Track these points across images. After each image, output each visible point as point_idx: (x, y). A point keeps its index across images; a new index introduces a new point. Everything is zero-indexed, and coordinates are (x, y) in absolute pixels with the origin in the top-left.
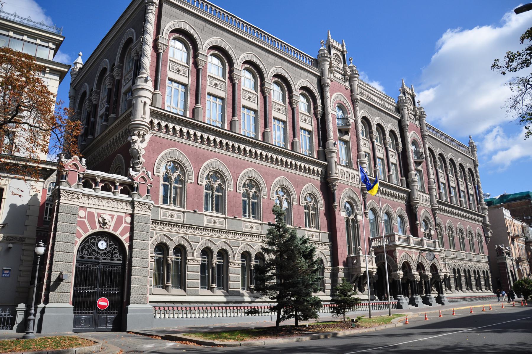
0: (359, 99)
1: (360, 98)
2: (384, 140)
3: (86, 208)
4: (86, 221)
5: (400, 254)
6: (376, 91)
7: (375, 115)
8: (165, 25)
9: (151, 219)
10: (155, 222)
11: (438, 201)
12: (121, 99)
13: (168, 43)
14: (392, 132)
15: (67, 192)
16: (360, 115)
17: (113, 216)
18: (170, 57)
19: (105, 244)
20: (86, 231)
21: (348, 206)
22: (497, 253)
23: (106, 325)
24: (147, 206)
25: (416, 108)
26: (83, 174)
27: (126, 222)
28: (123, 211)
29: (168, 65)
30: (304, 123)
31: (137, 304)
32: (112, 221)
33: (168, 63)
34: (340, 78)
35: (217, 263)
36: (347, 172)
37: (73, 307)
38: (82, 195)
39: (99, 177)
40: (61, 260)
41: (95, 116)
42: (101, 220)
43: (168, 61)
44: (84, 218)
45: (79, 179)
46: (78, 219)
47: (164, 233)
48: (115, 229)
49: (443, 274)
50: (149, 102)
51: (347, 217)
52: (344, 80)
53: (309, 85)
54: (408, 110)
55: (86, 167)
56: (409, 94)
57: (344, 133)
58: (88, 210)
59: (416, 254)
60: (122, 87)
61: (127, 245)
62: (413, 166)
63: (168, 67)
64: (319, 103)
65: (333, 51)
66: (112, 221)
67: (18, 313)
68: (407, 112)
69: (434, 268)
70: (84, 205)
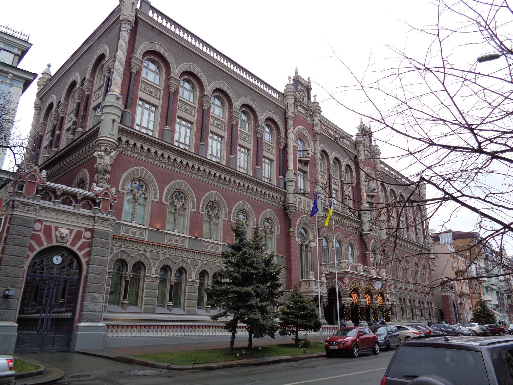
2: (340, 173)
4: (41, 234)
5: (350, 281)
7: (332, 150)
8: (140, 45)
10: (116, 238)
12: (90, 114)
13: (142, 64)
14: (348, 165)
15: (23, 204)
16: (319, 148)
17: (71, 231)
18: (142, 78)
19: (60, 259)
20: (40, 244)
21: (303, 231)
23: (53, 344)
24: (109, 222)
25: (372, 145)
26: (43, 186)
27: (85, 238)
29: (140, 85)
30: (267, 153)
32: (70, 235)
33: (140, 83)
35: (176, 281)
36: (304, 200)
37: (17, 325)
39: (60, 189)
40: (9, 275)
41: (60, 129)
43: (141, 81)
44: (40, 231)
45: (37, 190)
47: (123, 249)
48: (73, 244)
49: (390, 303)
50: (118, 120)
51: (301, 243)
53: (274, 117)
54: (364, 147)
55: (46, 180)
57: (303, 165)
58: (44, 223)
59: (365, 281)
60: (92, 102)
61: (84, 261)
63: (140, 87)
64: (283, 135)
65: (299, 87)
66: (70, 235)
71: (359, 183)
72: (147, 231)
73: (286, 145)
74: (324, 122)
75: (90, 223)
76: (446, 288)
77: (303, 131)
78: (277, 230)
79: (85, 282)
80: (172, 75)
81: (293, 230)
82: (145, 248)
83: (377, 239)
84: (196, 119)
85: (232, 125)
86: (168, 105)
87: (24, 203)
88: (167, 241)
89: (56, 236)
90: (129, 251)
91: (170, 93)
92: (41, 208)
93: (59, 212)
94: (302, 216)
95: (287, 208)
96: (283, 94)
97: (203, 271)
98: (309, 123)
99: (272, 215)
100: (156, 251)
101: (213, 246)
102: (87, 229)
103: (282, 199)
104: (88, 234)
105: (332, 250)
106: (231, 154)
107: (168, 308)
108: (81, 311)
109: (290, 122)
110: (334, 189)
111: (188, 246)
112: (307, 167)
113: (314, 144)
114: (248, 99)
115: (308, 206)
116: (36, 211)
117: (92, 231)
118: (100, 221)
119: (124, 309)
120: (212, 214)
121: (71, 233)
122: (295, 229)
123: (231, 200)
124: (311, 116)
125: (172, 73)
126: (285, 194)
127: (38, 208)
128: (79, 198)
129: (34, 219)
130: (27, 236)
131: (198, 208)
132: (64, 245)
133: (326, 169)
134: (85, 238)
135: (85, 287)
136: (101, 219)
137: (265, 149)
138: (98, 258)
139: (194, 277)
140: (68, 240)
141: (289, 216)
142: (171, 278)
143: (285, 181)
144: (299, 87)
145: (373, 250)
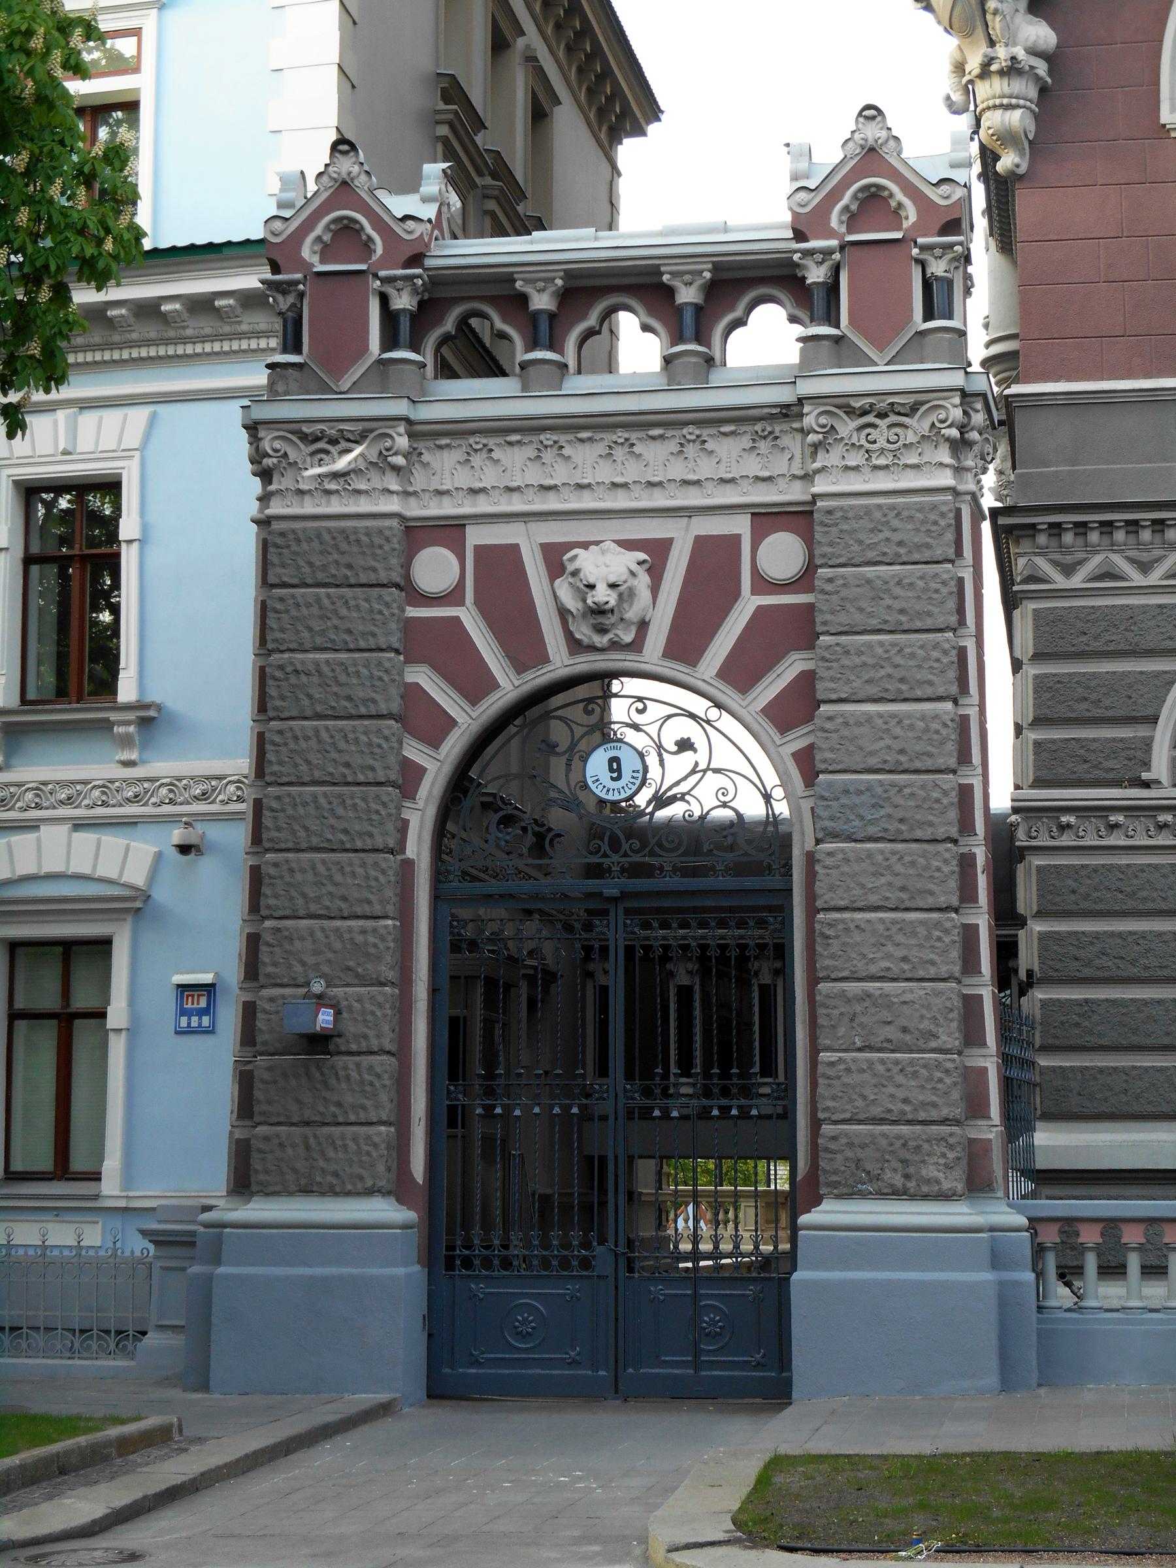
24: (920, 425)
27: (762, 584)
32: (655, 589)
40: (314, 908)
46: (413, 612)
58: (476, 536)
66: (655, 589)
70: (446, 508)
75: (779, 465)
82: (1120, 562)
87: (306, 429)
89: (564, 613)
93: (548, 438)
118: (847, 427)
121: (656, 572)
127: (403, 442)
128: (688, 295)
129: (394, 523)
134: (762, 584)
136: (851, 412)
138: (869, 718)
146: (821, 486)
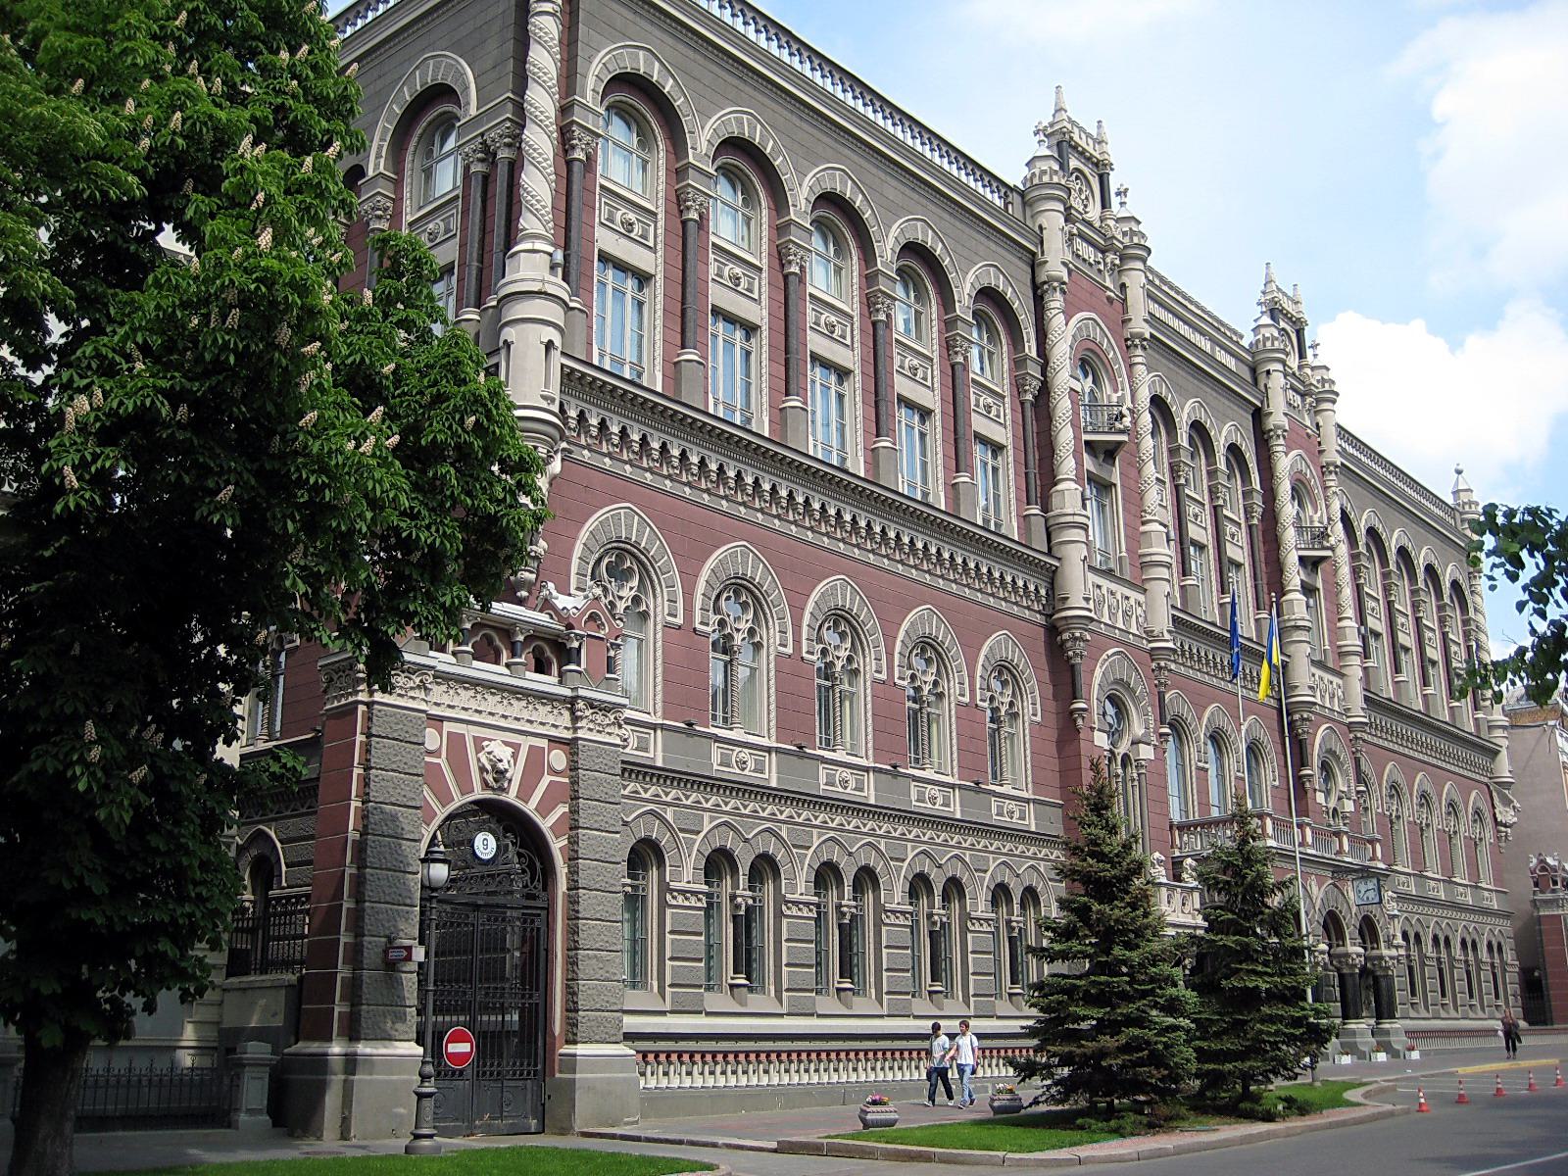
0: (1147, 336)
1: (1152, 335)
3: (441, 719)
4: (442, 761)
6: (1189, 306)
9: (623, 762)
11: (1367, 699)
14: (1234, 450)
17: (516, 747)
20: (444, 798)
21: (1110, 710)
22: (1536, 884)
27: (554, 772)
28: (541, 730)
31: (597, 1042)
33: (597, 197)
34: (1091, 261)
37: (420, 1050)
38: (435, 677)
40: (388, 899)
42: (484, 760)
46: (427, 759)
48: (525, 793)
51: (1111, 751)
52: (1102, 267)
56: (1286, 315)
57: (1102, 457)
61: (557, 845)
62: (1295, 576)
64: (1030, 347)
65: (1074, 163)
67: (248, 1074)
68: (1283, 381)
69: (1368, 930)
71: (1271, 517)
72: (659, 732)
73: (1045, 391)
74: (1160, 291)
76: (1554, 891)
77: (1095, 330)
78: (1033, 707)
79: (573, 916)
80: (691, 160)
81: (1083, 706)
83: (1334, 720)
84: (765, 313)
85: (874, 324)
86: (684, 270)
88: (716, 768)
90: (735, 821)
91: (684, 223)
92: (443, 677)
94: (1110, 652)
95: (1059, 624)
96: (1022, 194)
97: (824, 864)
98: (1109, 298)
99: (1013, 652)
100: (688, 803)
101: (846, 773)
102: (554, 741)
103: (1043, 592)
104: (558, 759)
105: (1237, 778)
106: (878, 436)
107: (1011, 1001)
108: (572, 1008)
109: (1055, 302)
110: (1194, 543)
111: (779, 778)
112: (1114, 465)
113: (1130, 376)
114: (919, 224)
115: (1125, 613)
116: (426, 689)
117: (571, 745)
119: (741, 1004)
120: (735, 635)
121: (515, 756)
122: (1088, 701)
123: (799, 578)
124: (1118, 270)
125: (690, 151)
126: (1052, 576)
130: (415, 771)
131: (797, 642)
132: (503, 797)
133: (1166, 465)
134: (554, 772)
135: (573, 931)
137: (977, 405)
139: (801, 887)
140: (510, 781)
141: (1071, 653)
142: (843, 903)
143: (1051, 522)
144: (1074, 163)
145: (1325, 767)
146: (580, 734)
